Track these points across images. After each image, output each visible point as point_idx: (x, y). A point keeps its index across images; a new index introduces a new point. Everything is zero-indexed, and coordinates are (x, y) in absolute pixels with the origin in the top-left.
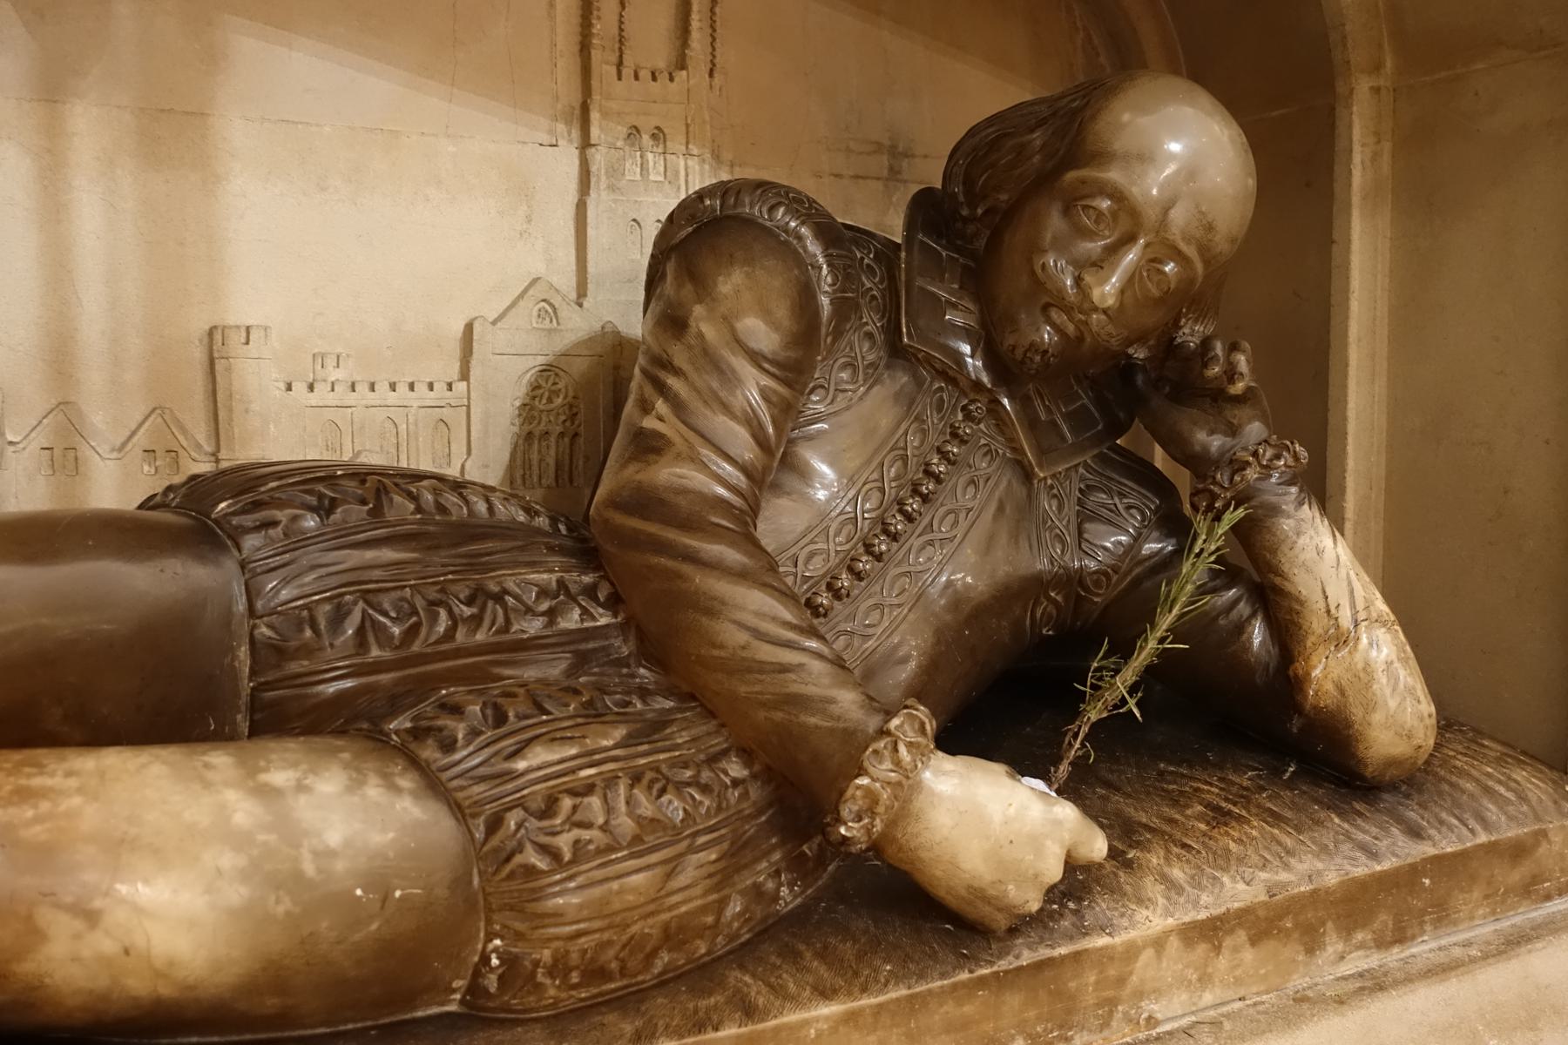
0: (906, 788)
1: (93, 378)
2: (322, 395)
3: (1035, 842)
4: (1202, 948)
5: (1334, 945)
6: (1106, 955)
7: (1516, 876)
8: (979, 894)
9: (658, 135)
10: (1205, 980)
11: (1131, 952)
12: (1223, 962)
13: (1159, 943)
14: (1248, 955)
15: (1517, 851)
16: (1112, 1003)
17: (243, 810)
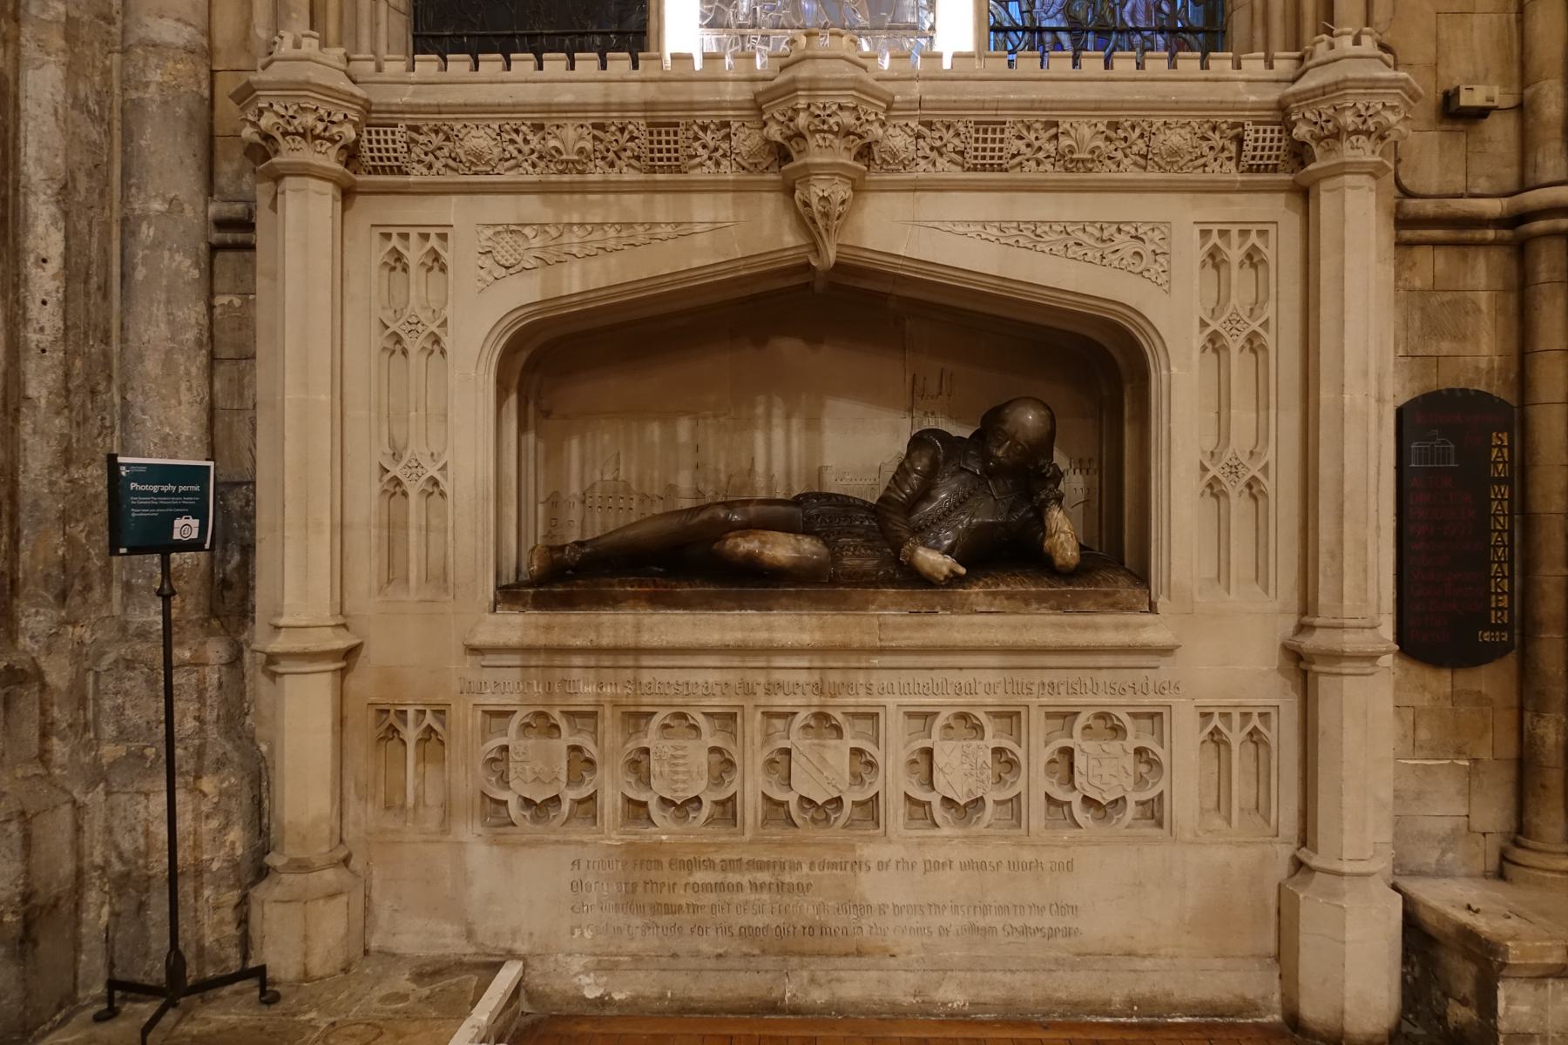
0: (913, 551)
1: (795, 478)
2: (844, 482)
3: (942, 564)
4: (990, 598)
5: (1035, 606)
6: (961, 594)
7: (1106, 601)
8: (929, 575)
9: (933, 413)
10: (991, 605)
11: (969, 594)
12: (997, 602)
13: (977, 594)
14: (1006, 602)
15: (1107, 594)
16: (964, 605)
17: (793, 541)
